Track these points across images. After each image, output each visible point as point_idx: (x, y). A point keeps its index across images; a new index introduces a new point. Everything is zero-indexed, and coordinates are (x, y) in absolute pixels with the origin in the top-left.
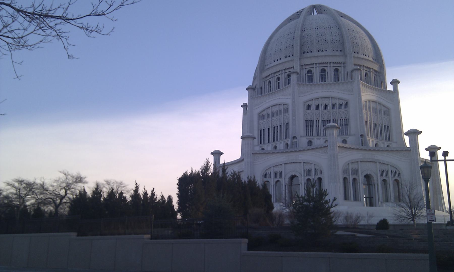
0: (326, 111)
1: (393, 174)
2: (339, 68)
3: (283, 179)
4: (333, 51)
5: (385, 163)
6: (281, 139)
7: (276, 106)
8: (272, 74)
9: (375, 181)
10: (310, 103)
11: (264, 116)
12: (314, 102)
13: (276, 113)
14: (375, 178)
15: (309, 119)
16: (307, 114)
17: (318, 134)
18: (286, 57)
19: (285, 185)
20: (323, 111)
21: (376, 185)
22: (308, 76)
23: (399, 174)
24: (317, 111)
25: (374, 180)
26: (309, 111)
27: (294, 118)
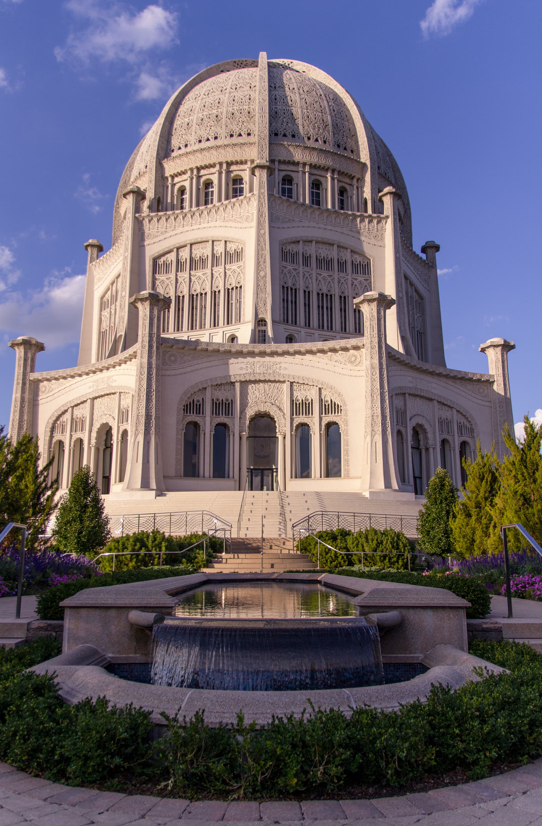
0: (325, 274)
1: (460, 428)
2: (348, 187)
3: (237, 420)
4: (339, 146)
5: (449, 403)
6: (215, 324)
9: (431, 442)
10: (294, 248)
11: (167, 266)
12: (300, 248)
13: (203, 261)
14: (430, 435)
15: (290, 285)
17: (308, 324)
18: (232, 136)
19: (240, 438)
20: (319, 271)
21: (431, 450)
22: (283, 190)
23: (472, 431)
24: (307, 269)
25: (426, 438)
26: (290, 267)
27: (262, 274)
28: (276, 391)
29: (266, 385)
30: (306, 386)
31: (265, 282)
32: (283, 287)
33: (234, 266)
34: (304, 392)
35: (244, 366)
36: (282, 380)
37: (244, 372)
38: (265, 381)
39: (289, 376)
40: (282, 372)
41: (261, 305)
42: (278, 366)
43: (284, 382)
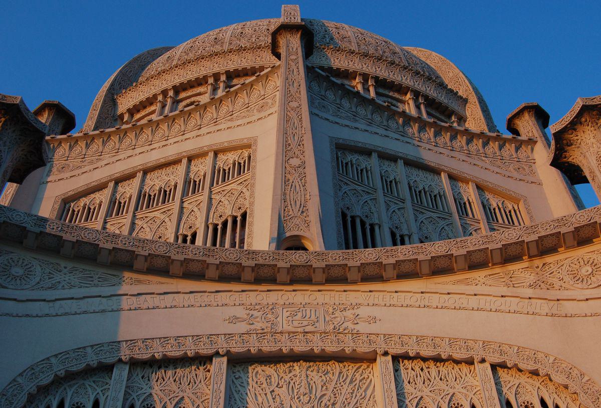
7: (170, 170)
8: (165, 93)
16: (345, 188)
27: (295, 162)
28: (346, 389)
29: (315, 374)
30: (444, 369)
31: (303, 176)
32: (344, 215)
33: (233, 186)
34: (442, 385)
35: (241, 312)
36: (363, 348)
37: (243, 327)
38: (309, 357)
39: (388, 337)
40: (362, 327)
41: (294, 211)
42: (349, 314)
43: (370, 359)
